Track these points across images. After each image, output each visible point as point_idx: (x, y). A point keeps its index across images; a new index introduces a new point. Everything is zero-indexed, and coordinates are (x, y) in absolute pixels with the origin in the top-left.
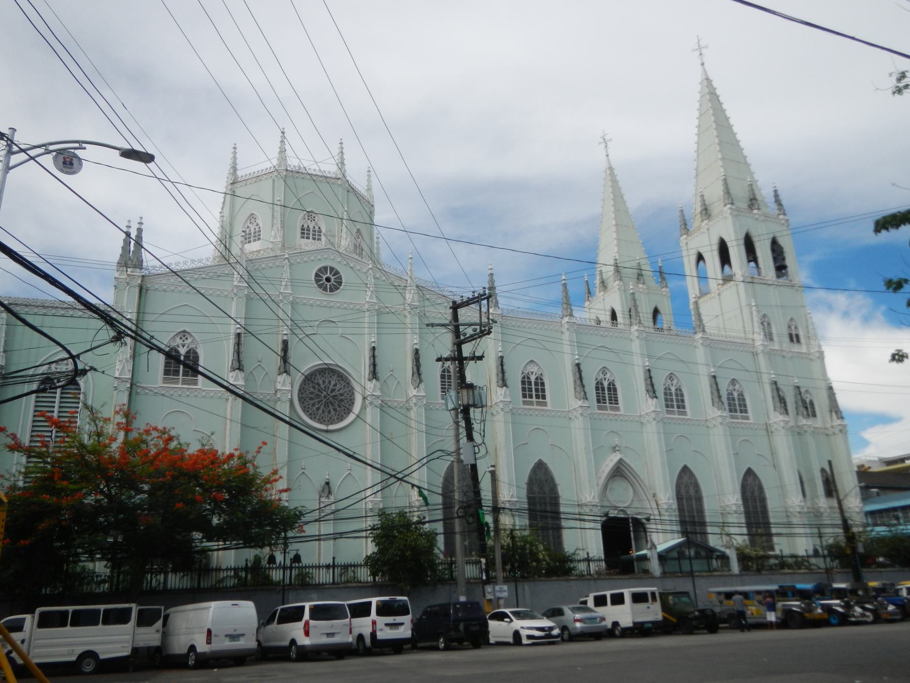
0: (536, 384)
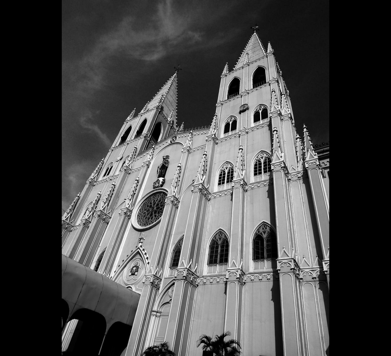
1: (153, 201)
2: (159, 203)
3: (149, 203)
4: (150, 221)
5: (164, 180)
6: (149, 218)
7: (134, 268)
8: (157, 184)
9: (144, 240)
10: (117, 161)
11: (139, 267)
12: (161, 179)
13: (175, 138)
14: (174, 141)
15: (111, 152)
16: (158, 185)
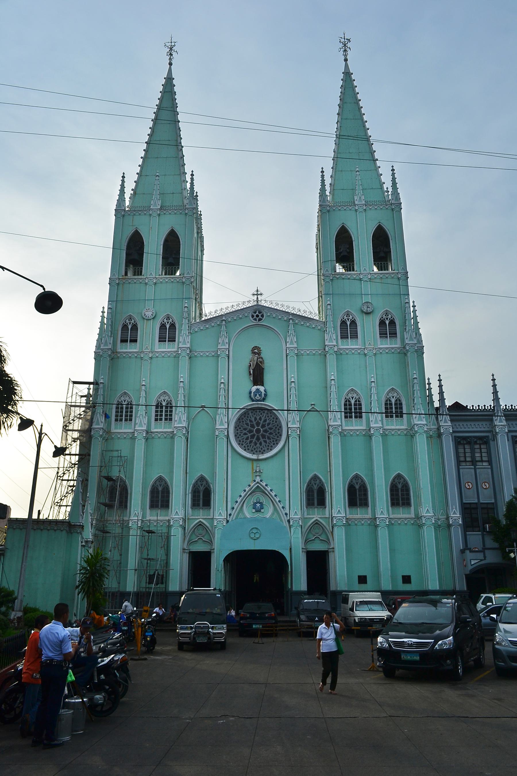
0: (396, 404)
1: (253, 419)
2: (265, 424)
3: (247, 420)
4: (259, 447)
5: (265, 391)
6: (256, 444)
7: (258, 505)
8: (258, 395)
9: (262, 472)
10: (146, 319)
11: (264, 503)
12: (262, 388)
13: (259, 313)
14: (260, 320)
15: (117, 289)
16: (259, 398)
